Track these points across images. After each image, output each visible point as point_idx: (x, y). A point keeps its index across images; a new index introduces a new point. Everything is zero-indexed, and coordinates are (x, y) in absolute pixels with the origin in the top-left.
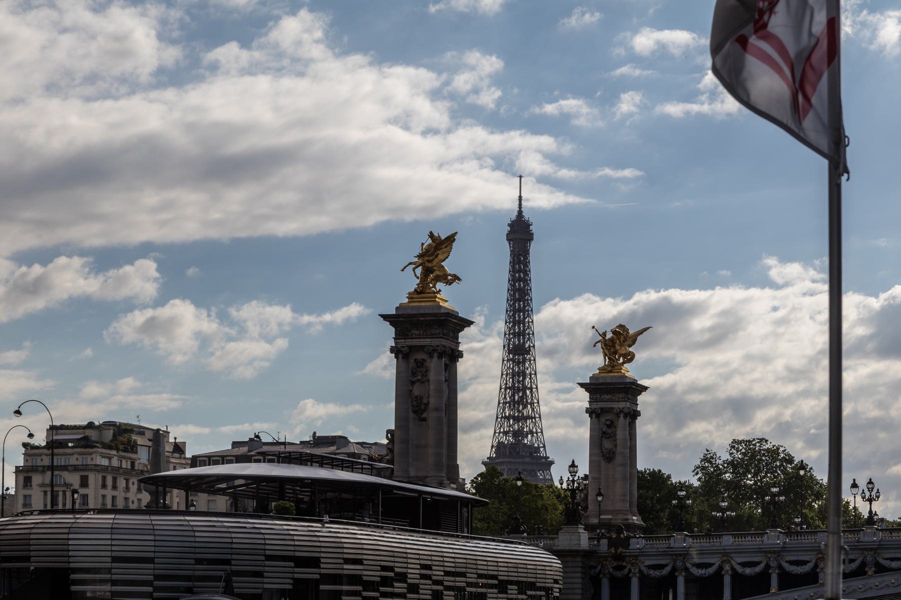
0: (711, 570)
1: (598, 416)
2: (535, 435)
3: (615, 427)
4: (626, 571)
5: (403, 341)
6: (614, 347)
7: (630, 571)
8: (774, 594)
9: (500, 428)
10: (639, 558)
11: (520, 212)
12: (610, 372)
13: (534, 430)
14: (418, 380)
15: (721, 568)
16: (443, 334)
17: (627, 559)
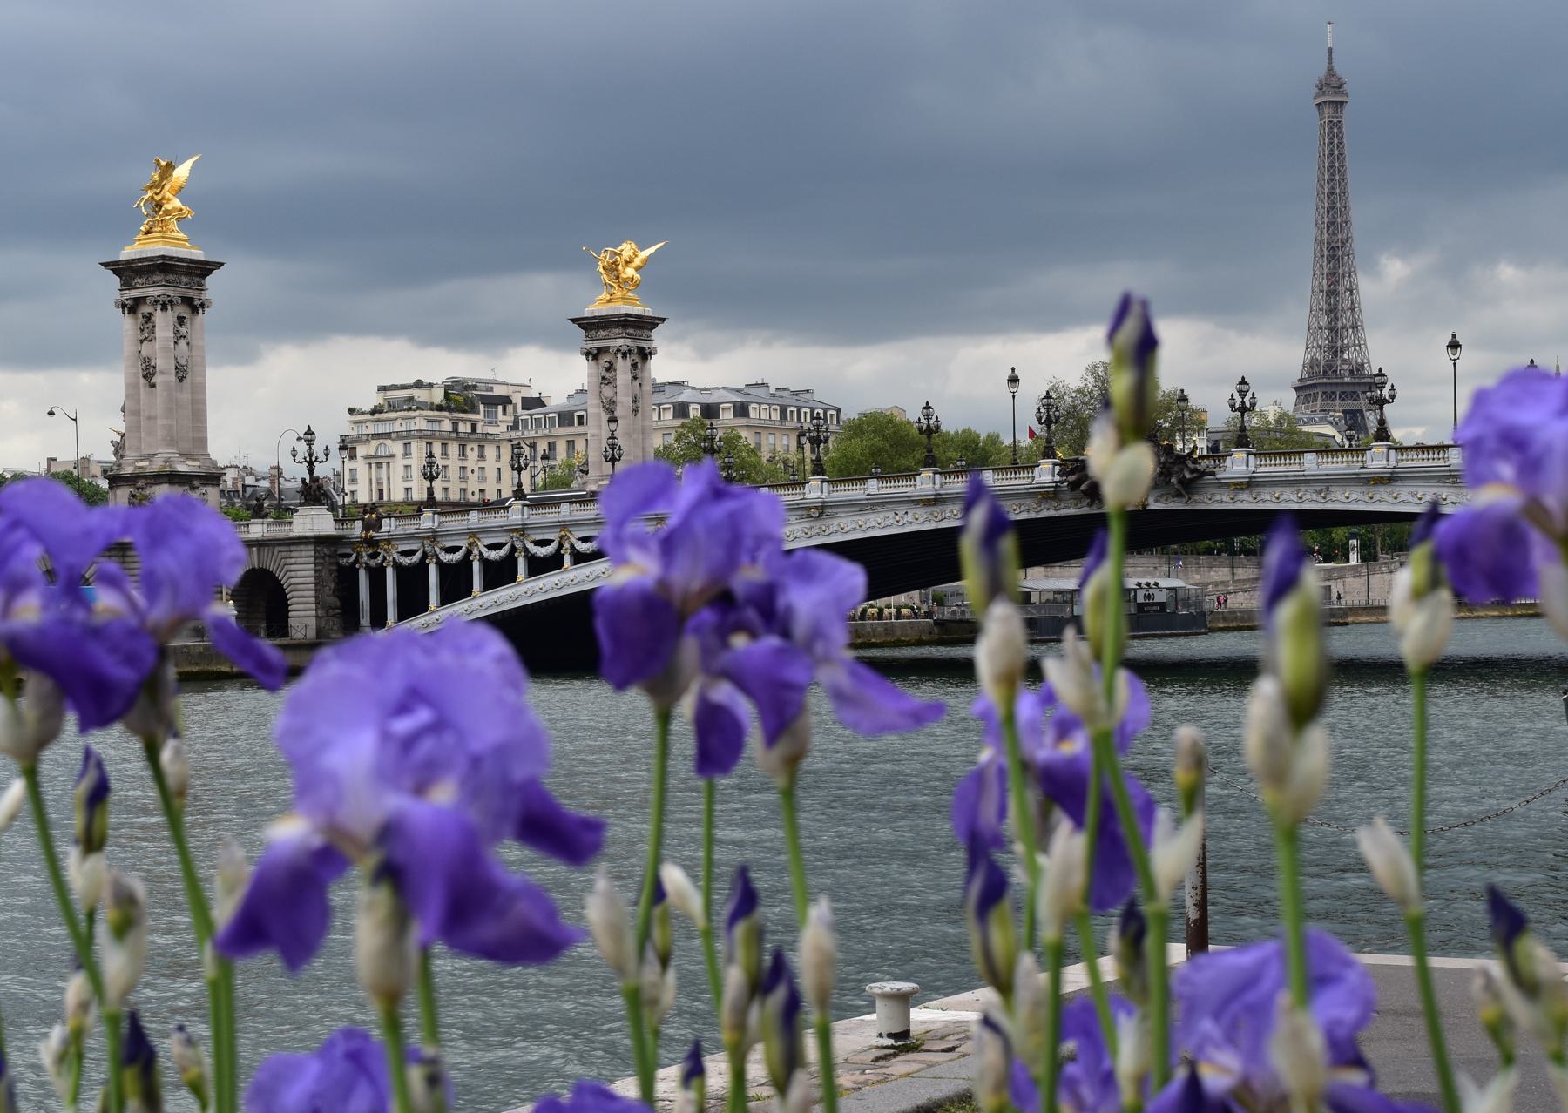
0: (458, 556)
1: (595, 358)
2: (1357, 348)
3: (615, 370)
4: (380, 559)
5: (127, 292)
6: (617, 270)
7: (385, 558)
8: (521, 583)
9: (1313, 342)
10: (393, 543)
11: (1330, 69)
12: (610, 301)
13: (1357, 342)
14: (146, 338)
15: (469, 552)
16: (166, 281)
17: (381, 544)
